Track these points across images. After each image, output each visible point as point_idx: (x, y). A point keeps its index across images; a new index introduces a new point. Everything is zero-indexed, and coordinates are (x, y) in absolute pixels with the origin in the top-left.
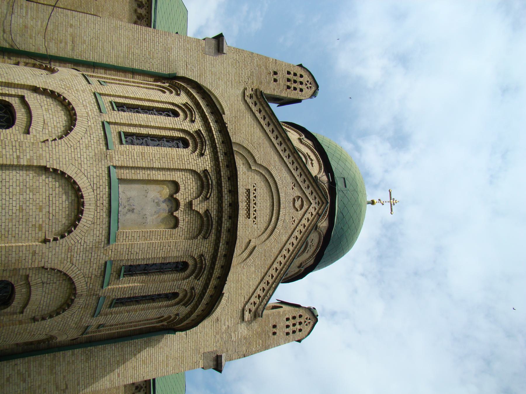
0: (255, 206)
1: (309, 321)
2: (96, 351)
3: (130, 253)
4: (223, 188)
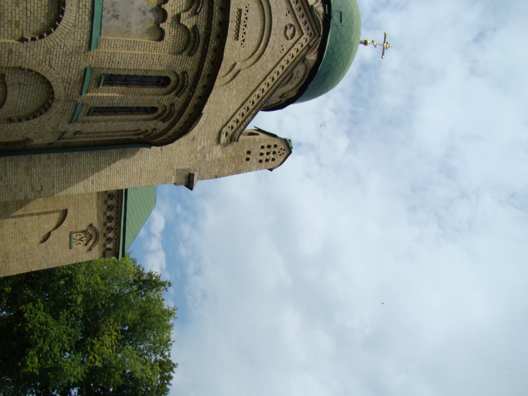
0: (245, 28)
3: (111, 62)
4: (215, 5)
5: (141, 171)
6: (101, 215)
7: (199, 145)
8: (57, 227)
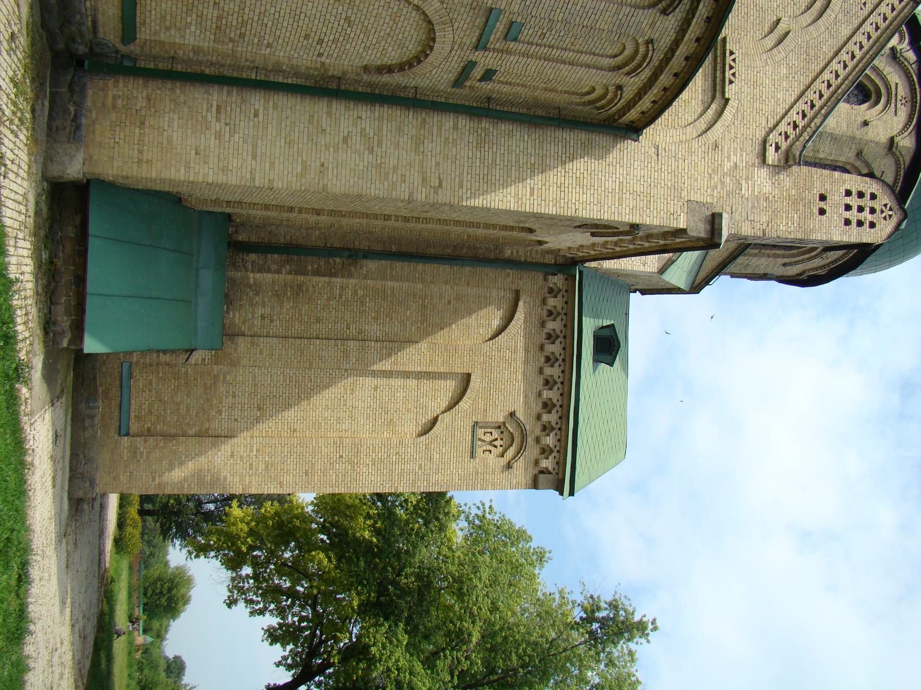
1: (891, 213)
2: (495, 134)
5: (621, 190)
6: (532, 397)
7: (726, 159)
8: (449, 408)
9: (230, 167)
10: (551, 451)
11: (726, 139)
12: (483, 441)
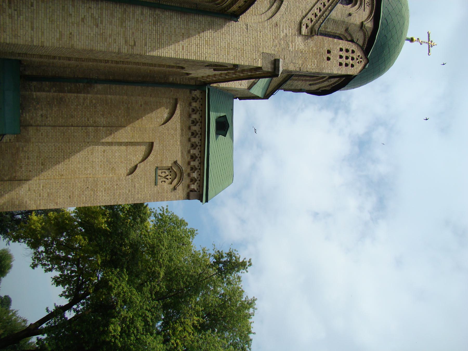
1: (361, 60)
6: (185, 153)
7: (281, 32)
8: (143, 160)
9: (19, 35)
10: (196, 180)
11: (282, 21)
12: (161, 176)
